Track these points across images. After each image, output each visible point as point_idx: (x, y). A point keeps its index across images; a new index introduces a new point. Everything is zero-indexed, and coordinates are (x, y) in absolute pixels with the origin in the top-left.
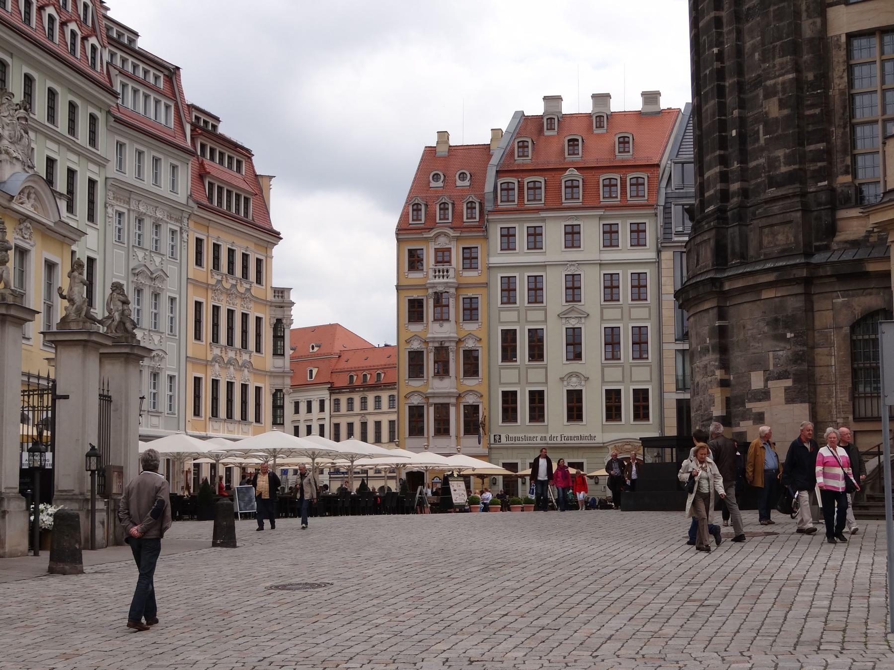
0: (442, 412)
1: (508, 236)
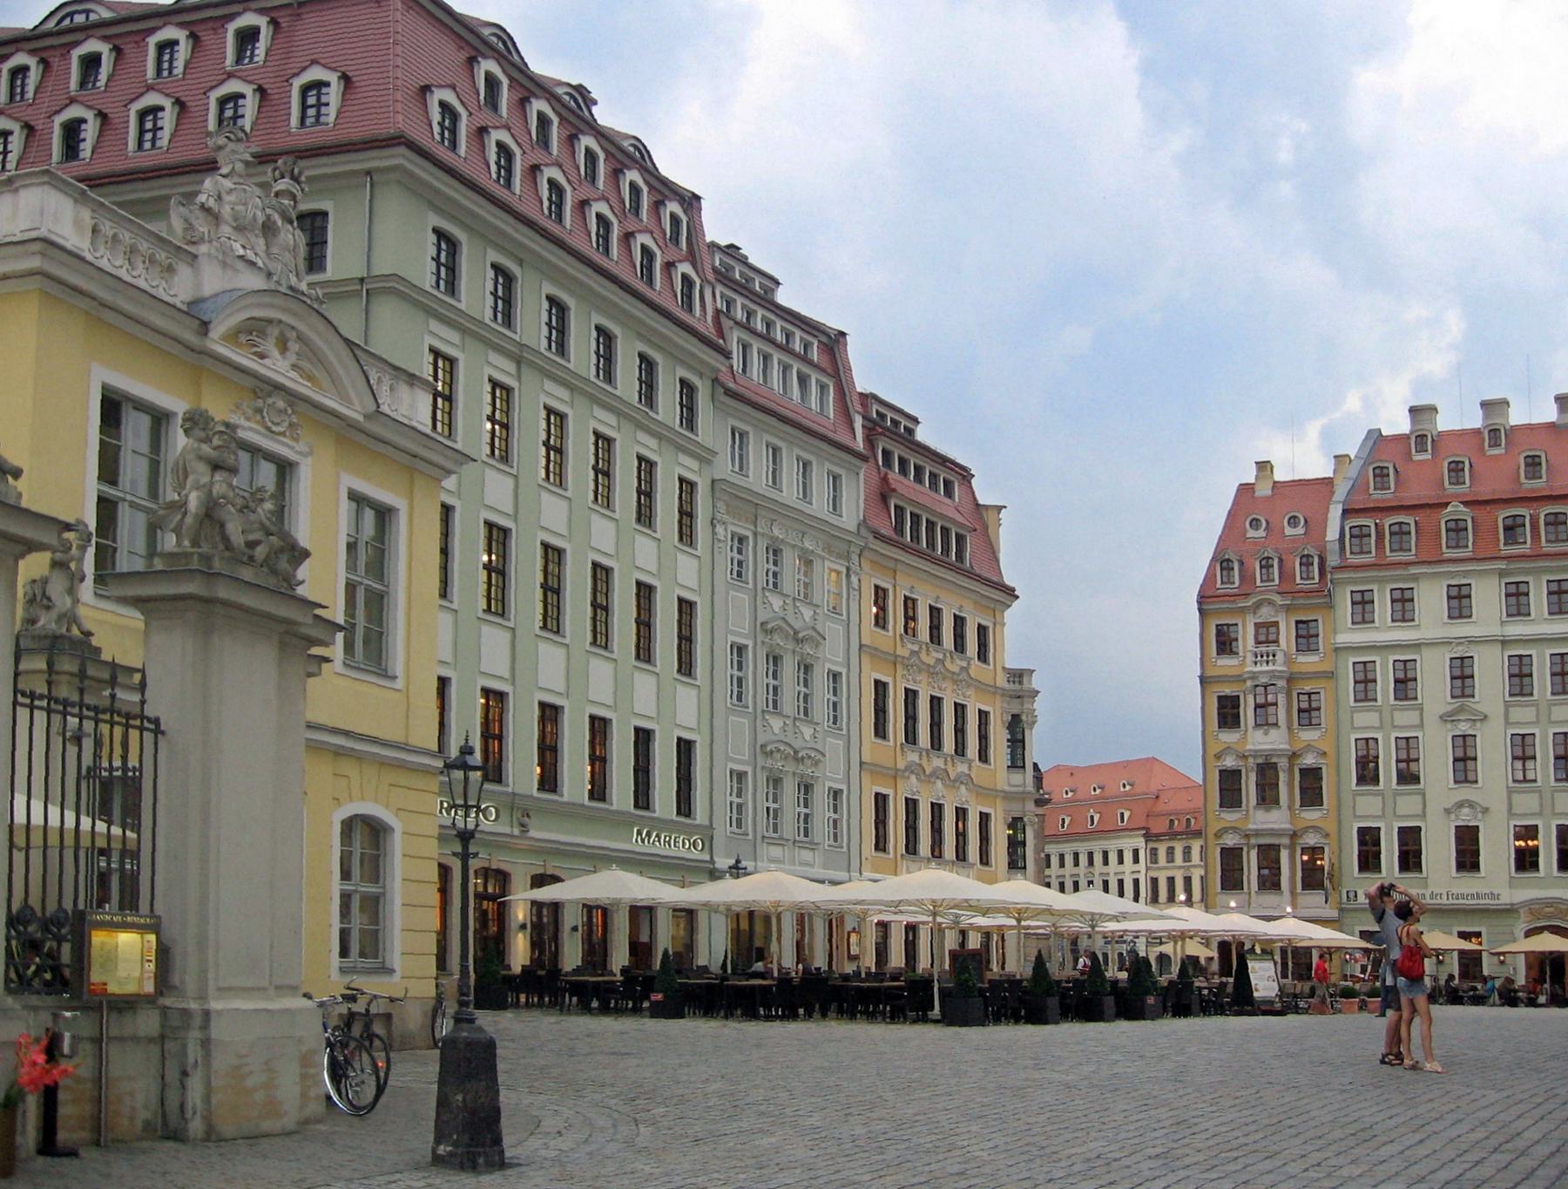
0: (1269, 856)
1: (1363, 603)
